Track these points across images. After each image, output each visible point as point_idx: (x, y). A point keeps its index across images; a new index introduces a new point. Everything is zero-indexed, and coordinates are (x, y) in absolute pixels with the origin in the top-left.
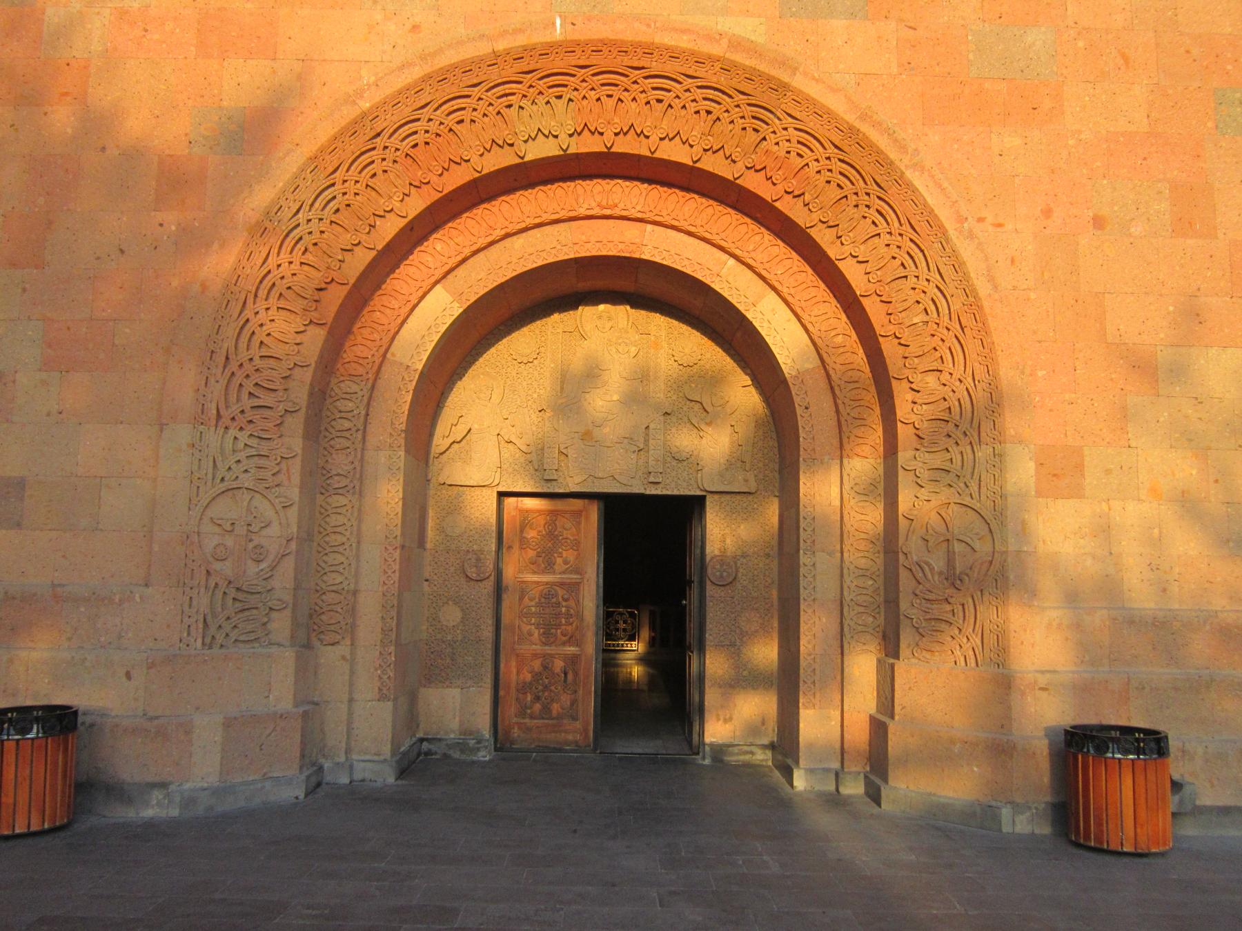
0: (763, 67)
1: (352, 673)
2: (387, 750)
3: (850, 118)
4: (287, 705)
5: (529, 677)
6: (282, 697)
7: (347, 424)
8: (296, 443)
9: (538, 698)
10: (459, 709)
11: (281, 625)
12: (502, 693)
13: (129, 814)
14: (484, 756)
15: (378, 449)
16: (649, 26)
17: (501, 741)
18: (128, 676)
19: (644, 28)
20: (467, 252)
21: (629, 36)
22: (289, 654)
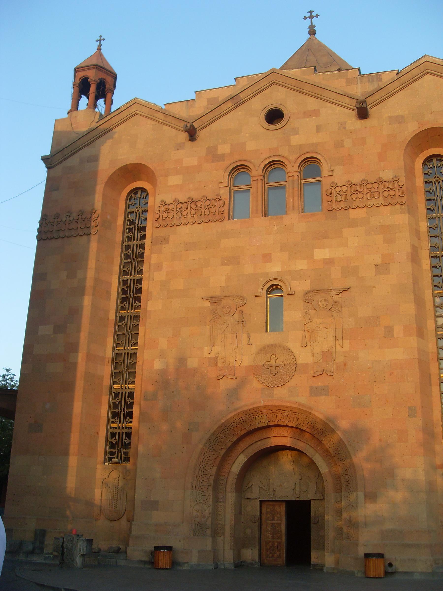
0: (305, 409)
1: (224, 543)
2: (232, 561)
3: (324, 419)
4: (210, 549)
5: (268, 547)
6: (209, 547)
7: (222, 487)
8: (211, 492)
9: (271, 553)
10: (250, 554)
11: (209, 532)
12: (262, 551)
13: (181, 568)
14: (256, 566)
15: (229, 492)
17: (262, 564)
18: (180, 541)
20: (247, 446)
21: (277, 404)
22: (210, 539)
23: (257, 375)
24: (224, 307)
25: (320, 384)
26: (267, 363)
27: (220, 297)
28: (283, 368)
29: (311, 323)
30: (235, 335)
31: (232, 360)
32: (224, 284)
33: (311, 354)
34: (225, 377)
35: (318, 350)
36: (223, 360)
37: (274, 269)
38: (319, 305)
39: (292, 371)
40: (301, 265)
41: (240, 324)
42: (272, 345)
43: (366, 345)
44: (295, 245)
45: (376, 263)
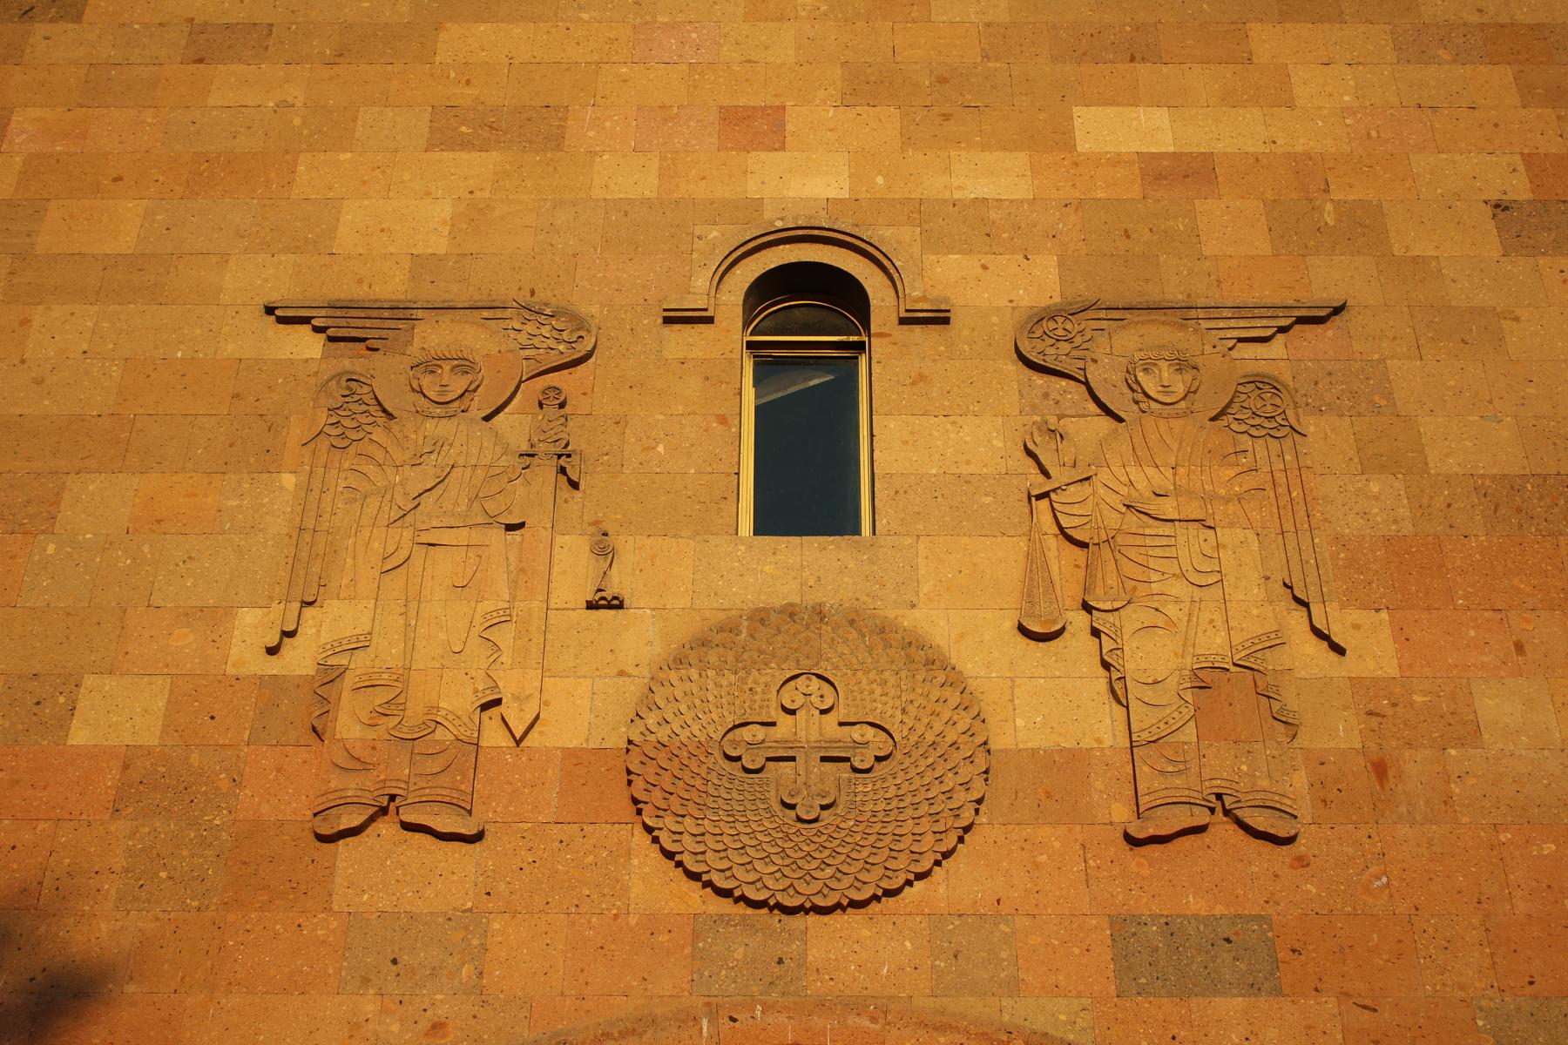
16: (874, 1019)
19: (867, 1023)
23: (660, 812)
24: (429, 366)
25: (1195, 904)
26: (746, 734)
27: (402, 313)
28: (881, 770)
29: (1086, 489)
30: (496, 536)
31: (458, 700)
32: (440, 245)
33: (1102, 685)
34: (386, 829)
35: (1153, 657)
36: (380, 697)
37: (808, 181)
38: (1133, 386)
39: (961, 797)
40: (991, 176)
41: (545, 473)
42: (790, 612)
43: (1519, 648)
44: (942, 80)
45: (1495, 196)
